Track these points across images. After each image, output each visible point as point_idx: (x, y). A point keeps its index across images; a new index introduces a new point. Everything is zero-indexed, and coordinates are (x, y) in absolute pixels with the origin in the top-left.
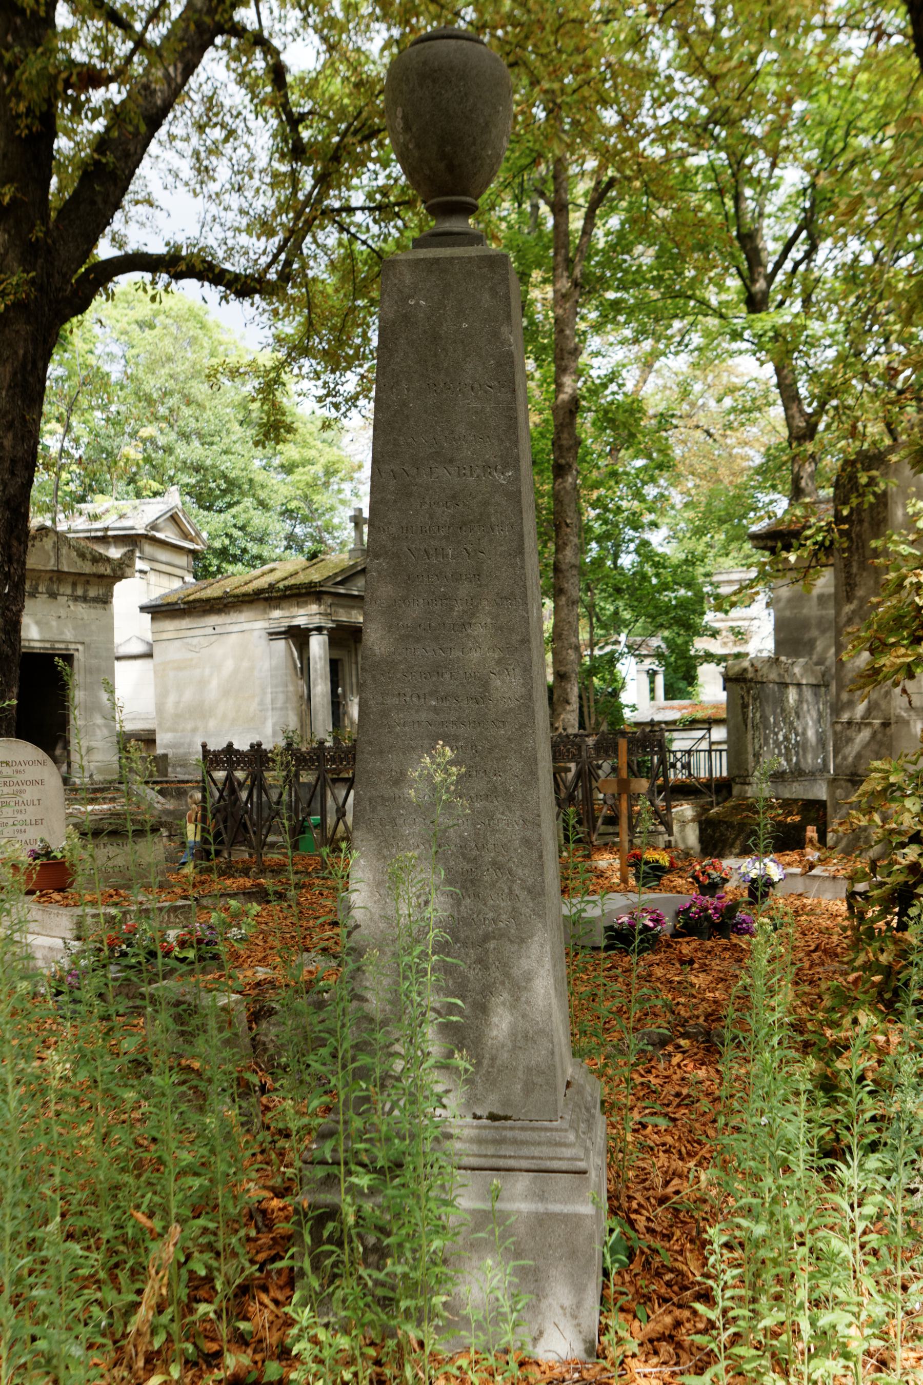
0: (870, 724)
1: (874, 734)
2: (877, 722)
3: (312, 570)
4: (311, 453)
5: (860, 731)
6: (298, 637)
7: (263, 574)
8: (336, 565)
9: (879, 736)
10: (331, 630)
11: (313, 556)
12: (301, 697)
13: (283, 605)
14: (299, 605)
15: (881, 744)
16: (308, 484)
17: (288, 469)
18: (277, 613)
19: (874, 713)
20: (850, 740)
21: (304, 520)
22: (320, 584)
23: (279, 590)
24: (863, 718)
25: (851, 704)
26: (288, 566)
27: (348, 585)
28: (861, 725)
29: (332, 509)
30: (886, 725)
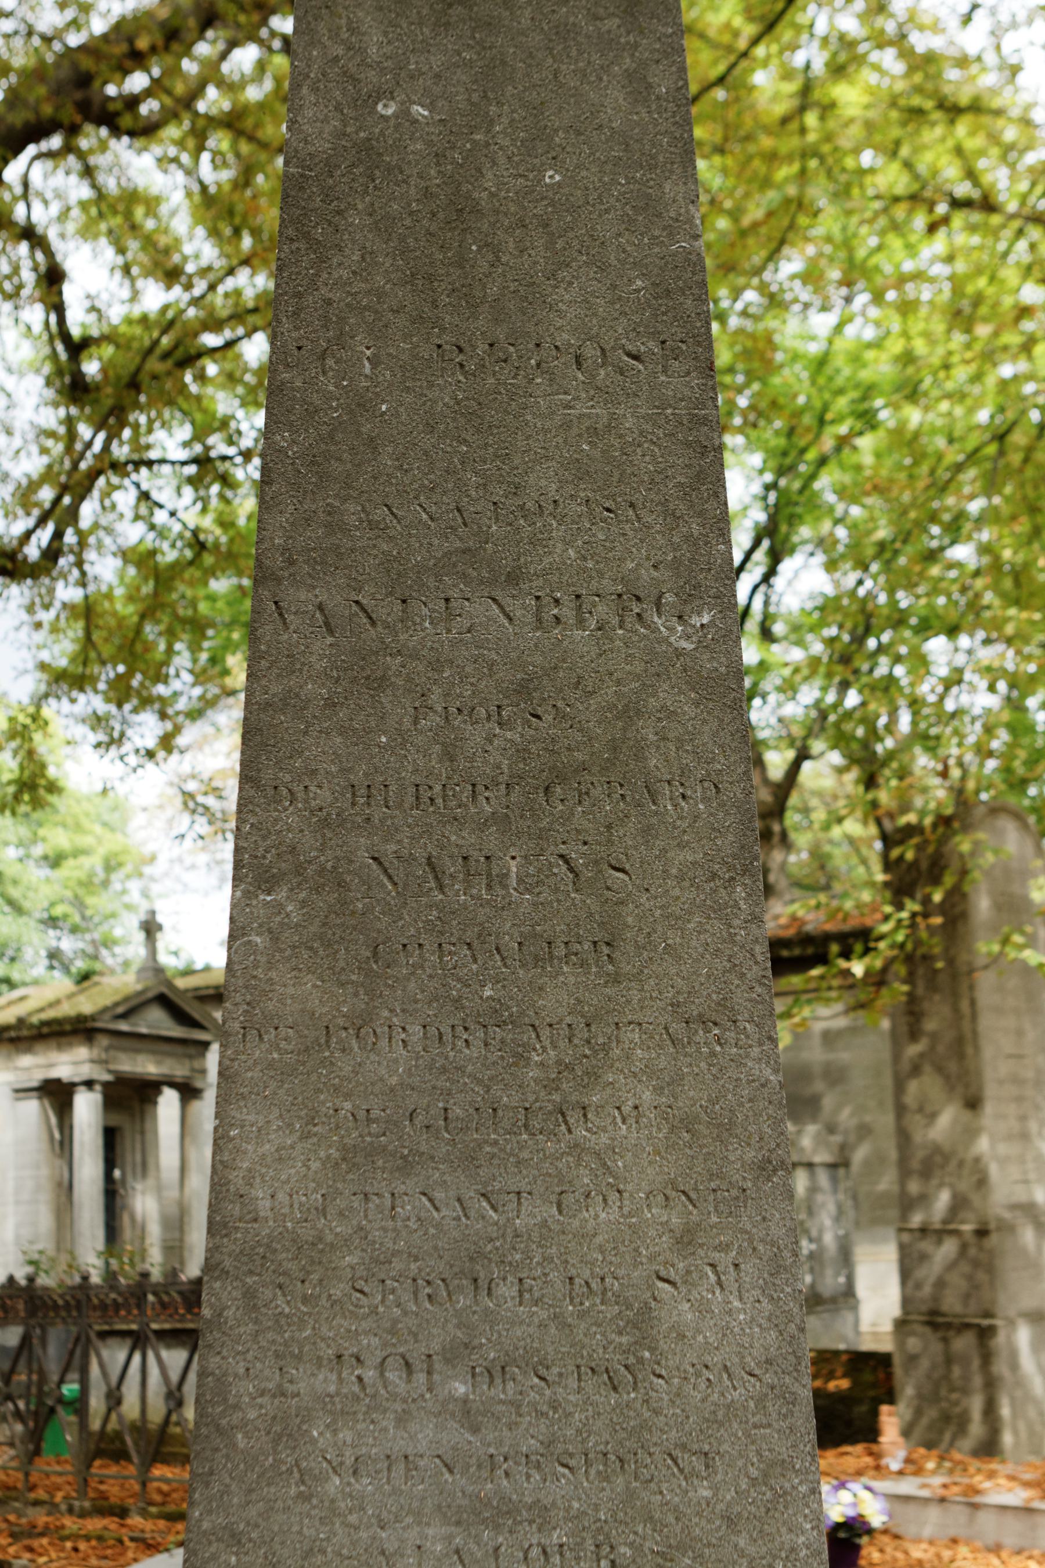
0: (956, 1233)
1: (964, 1247)
2: (967, 1228)
3: (82, 998)
4: (87, 841)
5: (939, 1242)
6: (57, 1094)
7: (10, 1004)
8: (116, 991)
9: (972, 1251)
10: (106, 1085)
11: (85, 977)
12: (60, 1185)
13: (39, 1047)
14: (60, 1048)
15: (976, 1264)
16: (81, 883)
17: (55, 861)
18: (26, 1060)
19: (962, 1215)
20: (924, 1257)
21: (74, 930)
22: (93, 1018)
23: (32, 1026)
24: (945, 1222)
25: (924, 1200)
26: (45, 992)
27: (134, 1019)
28: (941, 1234)
29: (113, 915)
30: (982, 1233)
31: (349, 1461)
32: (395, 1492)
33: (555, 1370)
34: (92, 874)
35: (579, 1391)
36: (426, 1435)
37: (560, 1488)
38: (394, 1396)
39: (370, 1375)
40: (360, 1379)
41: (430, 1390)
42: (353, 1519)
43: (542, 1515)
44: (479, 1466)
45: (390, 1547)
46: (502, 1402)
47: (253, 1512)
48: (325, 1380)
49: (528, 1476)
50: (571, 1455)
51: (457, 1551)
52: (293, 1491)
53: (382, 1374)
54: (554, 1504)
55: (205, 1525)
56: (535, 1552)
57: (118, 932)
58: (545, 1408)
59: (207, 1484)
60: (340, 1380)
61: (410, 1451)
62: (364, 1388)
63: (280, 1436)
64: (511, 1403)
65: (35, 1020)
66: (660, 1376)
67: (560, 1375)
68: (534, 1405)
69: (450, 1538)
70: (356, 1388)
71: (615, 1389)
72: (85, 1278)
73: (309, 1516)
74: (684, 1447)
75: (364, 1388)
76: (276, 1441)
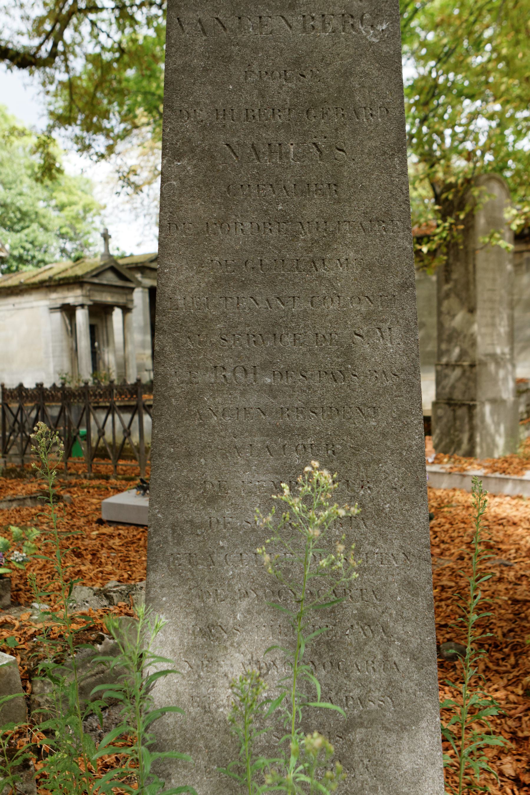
0: (462, 366)
1: (464, 372)
2: (466, 364)
3: (77, 268)
5: (454, 370)
6: (68, 311)
7: (45, 271)
8: (92, 265)
9: (468, 374)
10: (90, 307)
11: (77, 259)
12: (72, 349)
13: (59, 290)
14: (68, 290)
15: (469, 379)
18: (54, 296)
19: (464, 358)
20: (446, 376)
22: (82, 277)
23: (55, 281)
24: (456, 361)
25: (448, 351)
26: (60, 266)
27: (100, 277)
28: (454, 367)
30: (472, 366)
31: (220, 410)
32: (241, 423)
33: (310, 373)
34: (78, 214)
35: (320, 381)
36: (253, 400)
37: (311, 422)
38: (239, 384)
39: (229, 374)
40: (224, 376)
41: (255, 381)
42: (223, 434)
43: (303, 432)
44: (277, 413)
45: (239, 445)
46: (286, 386)
47: (180, 431)
48: (210, 377)
49: (298, 416)
50: (316, 408)
51: (267, 447)
52: (197, 422)
53: (234, 374)
54: (308, 428)
55: (160, 436)
56: (300, 447)
57: (91, 241)
58: (305, 389)
59: (160, 420)
60: (216, 376)
61: (247, 406)
62: (226, 380)
63: (191, 400)
64: (290, 386)
65: (57, 277)
66: (355, 375)
67: (312, 375)
68: (300, 387)
69: (264, 442)
70: (223, 380)
71: (335, 381)
72: (86, 383)
73: (204, 433)
74: (365, 405)
75: (226, 380)
76: (189, 402)
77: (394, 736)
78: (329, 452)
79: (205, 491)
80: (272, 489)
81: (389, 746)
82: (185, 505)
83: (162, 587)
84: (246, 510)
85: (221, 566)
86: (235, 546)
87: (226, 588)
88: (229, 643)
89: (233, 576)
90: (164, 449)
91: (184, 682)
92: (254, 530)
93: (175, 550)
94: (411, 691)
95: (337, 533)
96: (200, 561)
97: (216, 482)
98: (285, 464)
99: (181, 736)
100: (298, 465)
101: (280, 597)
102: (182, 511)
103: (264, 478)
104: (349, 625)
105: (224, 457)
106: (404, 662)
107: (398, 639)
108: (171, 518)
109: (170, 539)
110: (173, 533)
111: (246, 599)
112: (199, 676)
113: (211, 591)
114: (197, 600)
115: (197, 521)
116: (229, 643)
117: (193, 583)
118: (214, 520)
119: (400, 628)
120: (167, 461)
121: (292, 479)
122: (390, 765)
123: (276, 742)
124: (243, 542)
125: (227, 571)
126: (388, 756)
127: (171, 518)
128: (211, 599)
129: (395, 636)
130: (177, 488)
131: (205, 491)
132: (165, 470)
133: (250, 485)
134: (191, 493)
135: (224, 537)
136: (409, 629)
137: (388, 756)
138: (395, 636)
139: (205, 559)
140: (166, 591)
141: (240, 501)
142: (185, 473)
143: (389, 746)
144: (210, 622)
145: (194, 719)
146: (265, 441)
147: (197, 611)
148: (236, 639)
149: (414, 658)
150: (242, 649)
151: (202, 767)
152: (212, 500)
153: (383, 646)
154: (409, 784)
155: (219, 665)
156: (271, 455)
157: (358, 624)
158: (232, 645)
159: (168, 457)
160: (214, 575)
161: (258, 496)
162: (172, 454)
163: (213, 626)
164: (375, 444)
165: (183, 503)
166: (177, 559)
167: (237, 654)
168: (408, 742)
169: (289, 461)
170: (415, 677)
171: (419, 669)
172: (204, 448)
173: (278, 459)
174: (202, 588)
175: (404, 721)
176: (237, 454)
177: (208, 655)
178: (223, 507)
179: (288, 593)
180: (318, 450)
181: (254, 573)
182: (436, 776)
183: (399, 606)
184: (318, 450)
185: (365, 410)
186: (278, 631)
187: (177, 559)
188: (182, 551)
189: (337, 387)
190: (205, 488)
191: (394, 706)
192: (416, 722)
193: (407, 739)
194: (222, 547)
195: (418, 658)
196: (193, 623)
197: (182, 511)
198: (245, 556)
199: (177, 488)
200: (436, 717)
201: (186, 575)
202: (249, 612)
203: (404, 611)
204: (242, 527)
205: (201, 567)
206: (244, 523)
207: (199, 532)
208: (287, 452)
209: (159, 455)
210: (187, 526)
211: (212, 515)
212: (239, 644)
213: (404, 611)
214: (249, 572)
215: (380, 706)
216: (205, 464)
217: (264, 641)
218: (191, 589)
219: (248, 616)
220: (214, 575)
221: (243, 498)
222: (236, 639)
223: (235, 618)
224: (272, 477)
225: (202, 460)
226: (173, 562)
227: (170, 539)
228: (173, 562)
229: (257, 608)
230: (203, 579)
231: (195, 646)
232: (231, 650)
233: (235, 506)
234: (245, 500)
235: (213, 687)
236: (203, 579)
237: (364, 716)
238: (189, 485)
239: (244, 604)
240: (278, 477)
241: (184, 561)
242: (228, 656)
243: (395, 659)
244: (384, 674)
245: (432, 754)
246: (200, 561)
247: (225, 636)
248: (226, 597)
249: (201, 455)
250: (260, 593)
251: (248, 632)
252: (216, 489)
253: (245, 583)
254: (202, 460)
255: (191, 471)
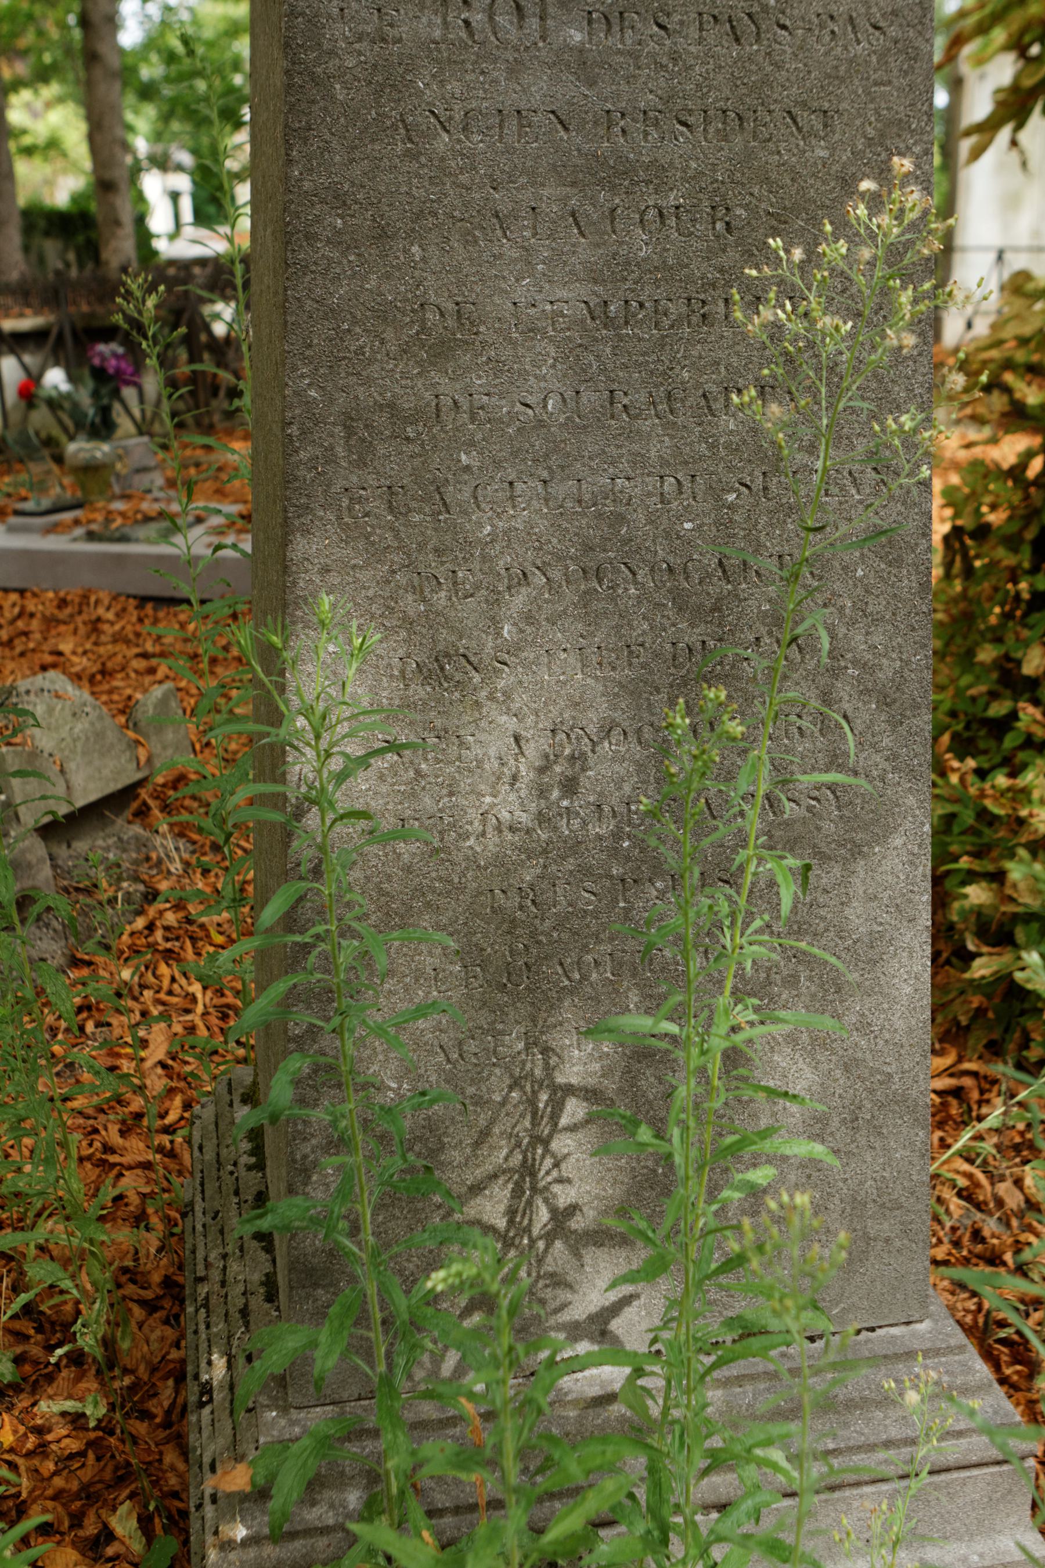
31: (458, 116)
32: (509, 150)
33: (676, 17)
35: (700, 41)
36: (539, 89)
37: (679, 149)
38: (504, 44)
39: (478, 18)
40: (467, 23)
41: (543, 38)
42: (464, 178)
43: (658, 176)
44: (596, 123)
45: (504, 209)
46: (619, 52)
47: (356, 171)
48: (430, 24)
49: (646, 134)
50: (690, 112)
51: (573, 214)
52: (400, 148)
53: (491, 18)
54: (671, 163)
55: (307, 185)
56: (652, 213)
58: (665, 61)
59: (305, 140)
60: (445, 23)
61: (523, 105)
62: (471, 34)
63: (382, 86)
64: (630, 54)
66: (783, 27)
67: (682, 23)
68: (652, 55)
69: (564, 200)
70: (463, 34)
71: (737, 40)
73: (418, 176)
74: (804, 104)
75: (471, 34)
76: (378, 93)
77: (837, 871)
78: (719, 225)
79: (423, 329)
80: (583, 321)
81: (826, 891)
82: (376, 367)
83: (326, 570)
84: (523, 374)
85: (466, 513)
86: (498, 464)
87: (476, 566)
88: (484, 694)
89: (493, 538)
90: (318, 220)
91: (384, 789)
92: (541, 424)
93: (354, 479)
94: (875, 773)
95: (732, 426)
96: (414, 504)
97: (451, 306)
98: (615, 255)
99: (379, 908)
100: (644, 260)
101: (600, 582)
102: (368, 382)
103: (564, 294)
104: (752, 638)
105: (469, 240)
106: (866, 711)
107: (855, 662)
108: (341, 398)
109: (340, 451)
110: (348, 438)
111: (523, 590)
112: (418, 772)
113: (441, 573)
114: (410, 598)
115: (407, 404)
116: (484, 694)
117: (397, 558)
118: (446, 401)
119: (859, 637)
120: (327, 251)
121: (630, 296)
122: (827, 930)
123: (588, 904)
124: (515, 454)
125: (480, 525)
126: (822, 912)
127: (341, 398)
128: (443, 594)
129: (849, 656)
130: (355, 322)
131: (423, 329)
132: (324, 274)
133: (532, 311)
134: (389, 334)
135: (472, 444)
136: (877, 639)
137: (822, 912)
138: (849, 656)
139: (426, 499)
140: (334, 579)
141: (507, 353)
142: (372, 284)
143: (826, 891)
144: (440, 647)
145: (408, 869)
146: (568, 197)
147: (408, 623)
148: (501, 684)
149: (885, 702)
150: (515, 706)
151: (429, 970)
152: (441, 352)
153: (822, 681)
154: (861, 965)
155: (462, 744)
156: (582, 234)
157: (770, 633)
158: (491, 698)
159: (329, 241)
160: (448, 537)
161: (551, 339)
162: (339, 232)
163: (447, 655)
164: (823, 206)
165: (371, 361)
166: (360, 500)
167: (505, 718)
168: (863, 881)
169: (623, 251)
170: (886, 742)
171: (895, 724)
172: (419, 216)
173: (598, 245)
174: (421, 569)
175: (859, 836)
176: (499, 233)
177: (438, 723)
178: (468, 369)
179: (619, 571)
180: (694, 220)
181: (542, 526)
182: (916, 944)
183: (860, 591)
184: (694, 220)
185: (804, 117)
186: (595, 659)
187: (360, 500)
188: (371, 480)
189: (740, 58)
190: (423, 321)
191: (839, 808)
192: (882, 839)
193: (862, 874)
194: (467, 468)
195: (894, 701)
196: (401, 652)
197: (368, 382)
198: (519, 486)
199: (355, 322)
200: (923, 824)
201: (383, 538)
202: (529, 618)
203: (870, 599)
204: (513, 416)
205: (417, 518)
206: (519, 407)
207: (410, 432)
208: (619, 227)
209: (307, 237)
210: (381, 419)
211: (441, 389)
212: (507, 695)
213: (870, 599)
214: (530, 525)
215: (810, 809)
216: (423, 259)
217: (565, 683)
218: (394, 572)
219: (529, 630)
220: (448, 537)
221: (514, 343)
222: (501, 684)
223: (498, 634)
224: (583, 290)
225: (415, 249)
226: (350, 509)
227: (340, 451)
228: (350, 509)
229: (548, 609)
230: (421, 547)
231: (407, 705)
232: (490, 709)
233: (497, 366)
234: (521, 351)
235: (451, 794)
236: (421, 547)
237: (778, 833)
238: (383, 314)
239: (519, 601)
240: (600, 289)
241: (377, 505)
242: (483, 724)
243: (846, 706)
244: (821, 742)
245: (910, 901)
246: (414, 504)
247: (477, 678)
248: (477, 587)
249: (411, 236)
250: (556, 574)
251: (526, 665)
252: (450, 323)
253: (521, 551)
254: (415, 249)
255: (388, 276)
